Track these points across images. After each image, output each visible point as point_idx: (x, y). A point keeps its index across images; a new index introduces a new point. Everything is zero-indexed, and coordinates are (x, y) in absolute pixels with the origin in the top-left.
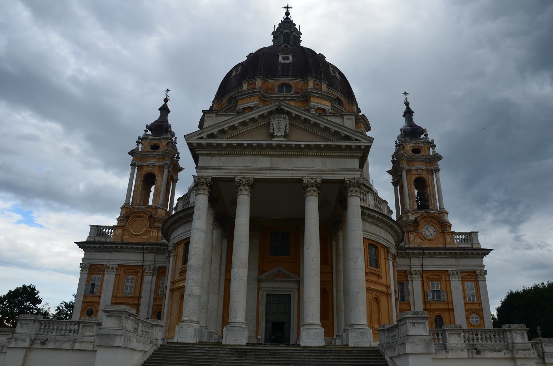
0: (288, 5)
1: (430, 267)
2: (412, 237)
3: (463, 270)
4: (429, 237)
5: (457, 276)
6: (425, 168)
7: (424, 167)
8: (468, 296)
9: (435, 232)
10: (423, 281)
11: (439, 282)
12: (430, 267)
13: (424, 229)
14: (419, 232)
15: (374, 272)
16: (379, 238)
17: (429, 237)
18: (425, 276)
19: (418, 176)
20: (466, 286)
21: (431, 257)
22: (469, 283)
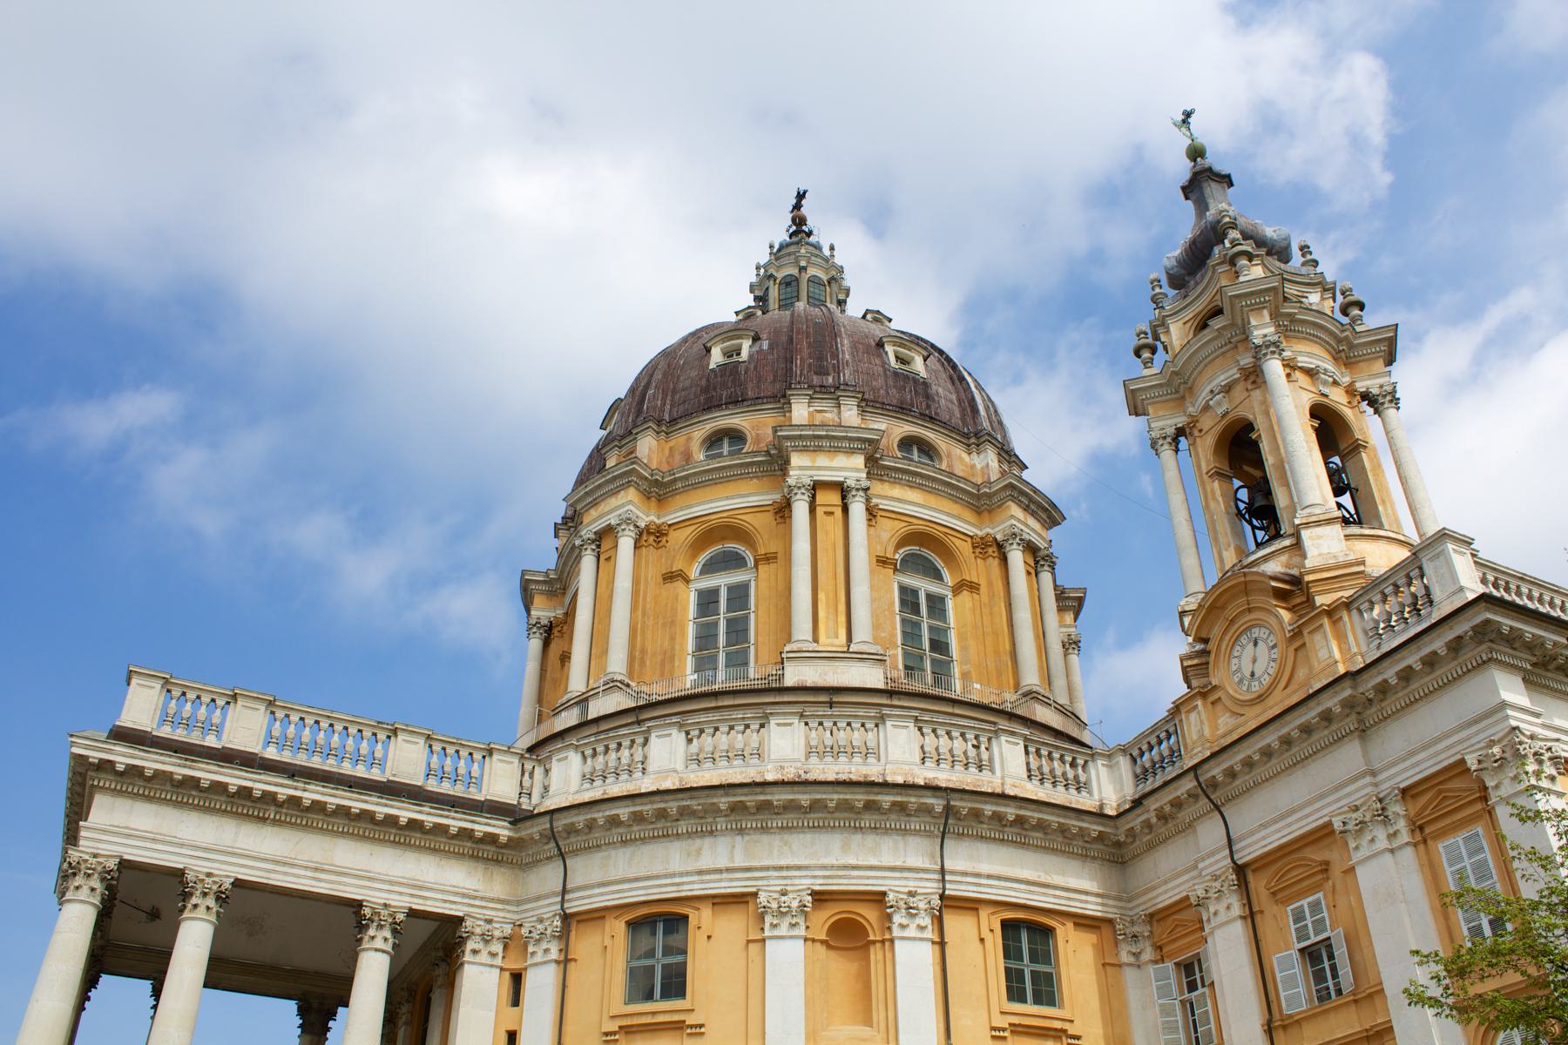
0: (799, 193)
1: (1264, 838)
2: (1196, 726)
3: (1402, 786)
4: (1257, 688)
5: (1380, 833)
6: (1234, 373)
7: (1231, 372)
8: (1468, 921)
9: (1274, 646)
10: (1251, 916)
11: (1320, 895)
12: (1264, 838)
13: (1235, 661)
14: (1215, 688)
15: (649, 1020)
16: (677, 880)
17: (1257, 688)
18: (1258, 884)
19: (1219, 428)
20: (1446, 865)
21: (1257, 785)
22: (1458, 839)
